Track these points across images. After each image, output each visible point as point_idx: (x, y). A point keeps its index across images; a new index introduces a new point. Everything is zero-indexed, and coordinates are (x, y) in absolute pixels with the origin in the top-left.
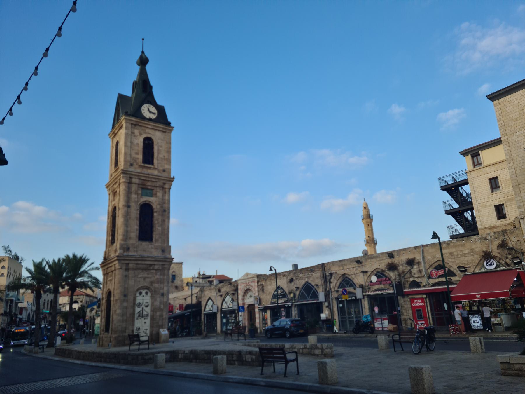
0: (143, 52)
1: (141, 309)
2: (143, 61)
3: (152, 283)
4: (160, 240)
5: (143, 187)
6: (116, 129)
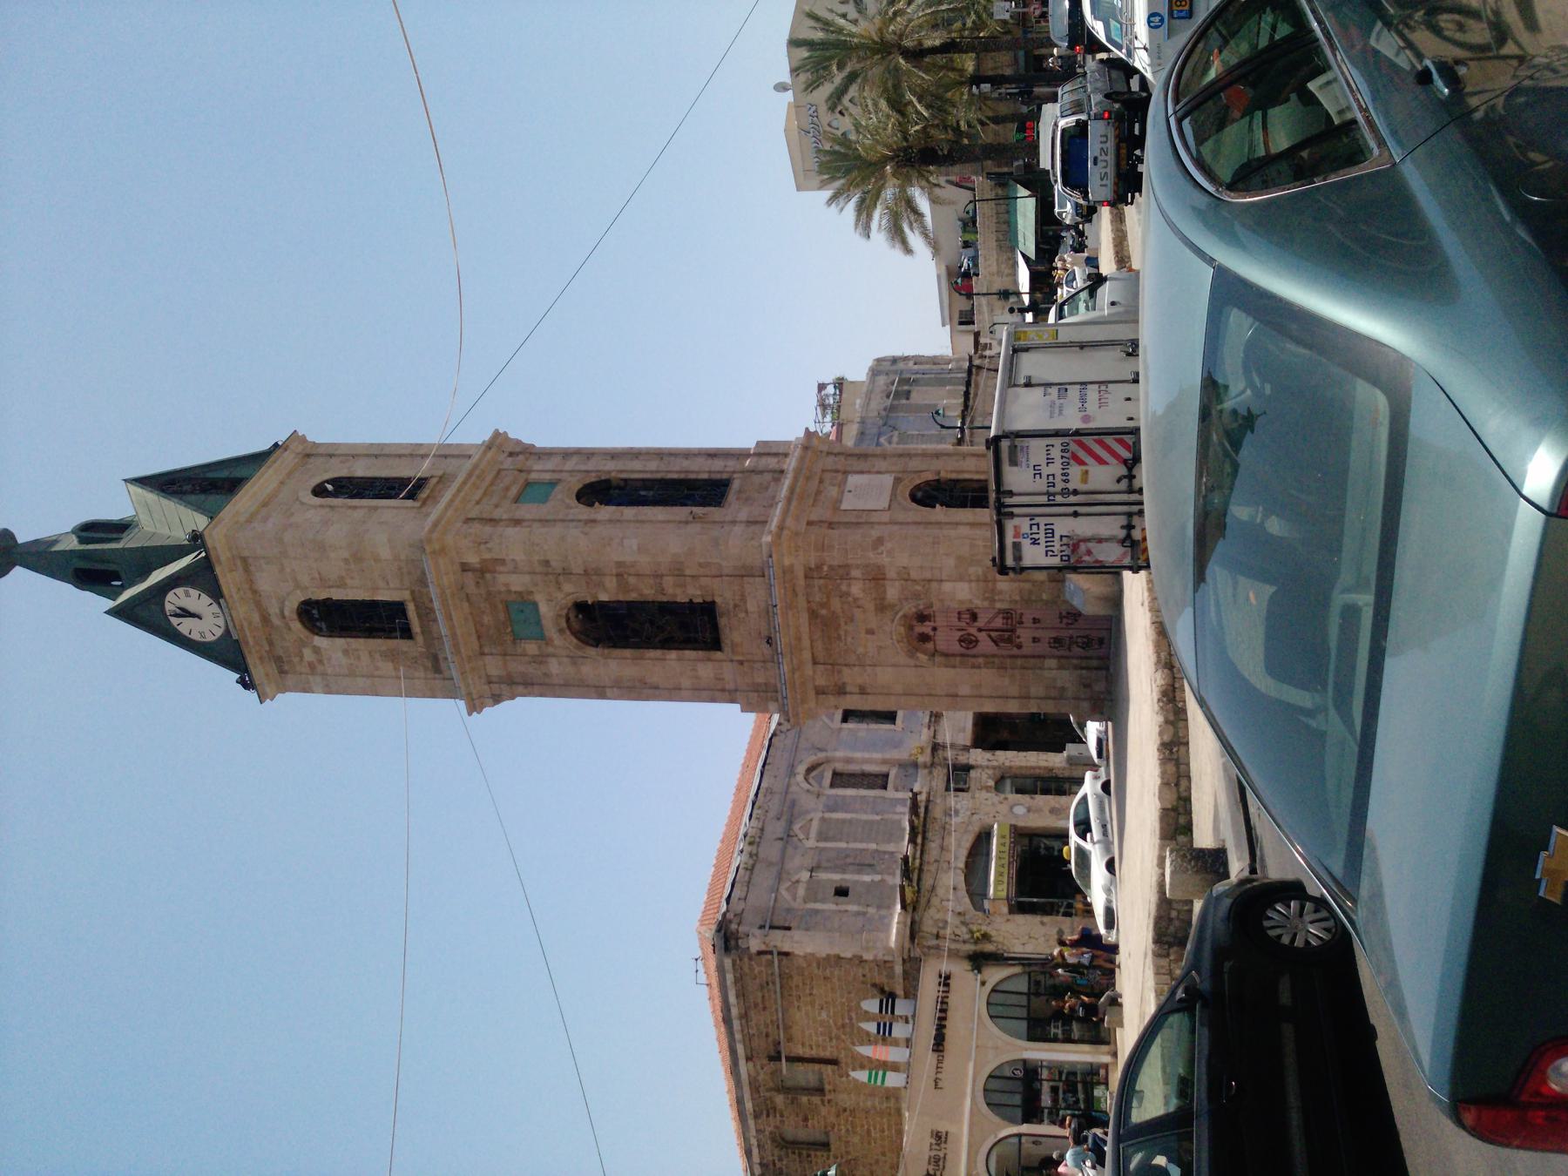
3: (882, 607)
5: (508, 638)
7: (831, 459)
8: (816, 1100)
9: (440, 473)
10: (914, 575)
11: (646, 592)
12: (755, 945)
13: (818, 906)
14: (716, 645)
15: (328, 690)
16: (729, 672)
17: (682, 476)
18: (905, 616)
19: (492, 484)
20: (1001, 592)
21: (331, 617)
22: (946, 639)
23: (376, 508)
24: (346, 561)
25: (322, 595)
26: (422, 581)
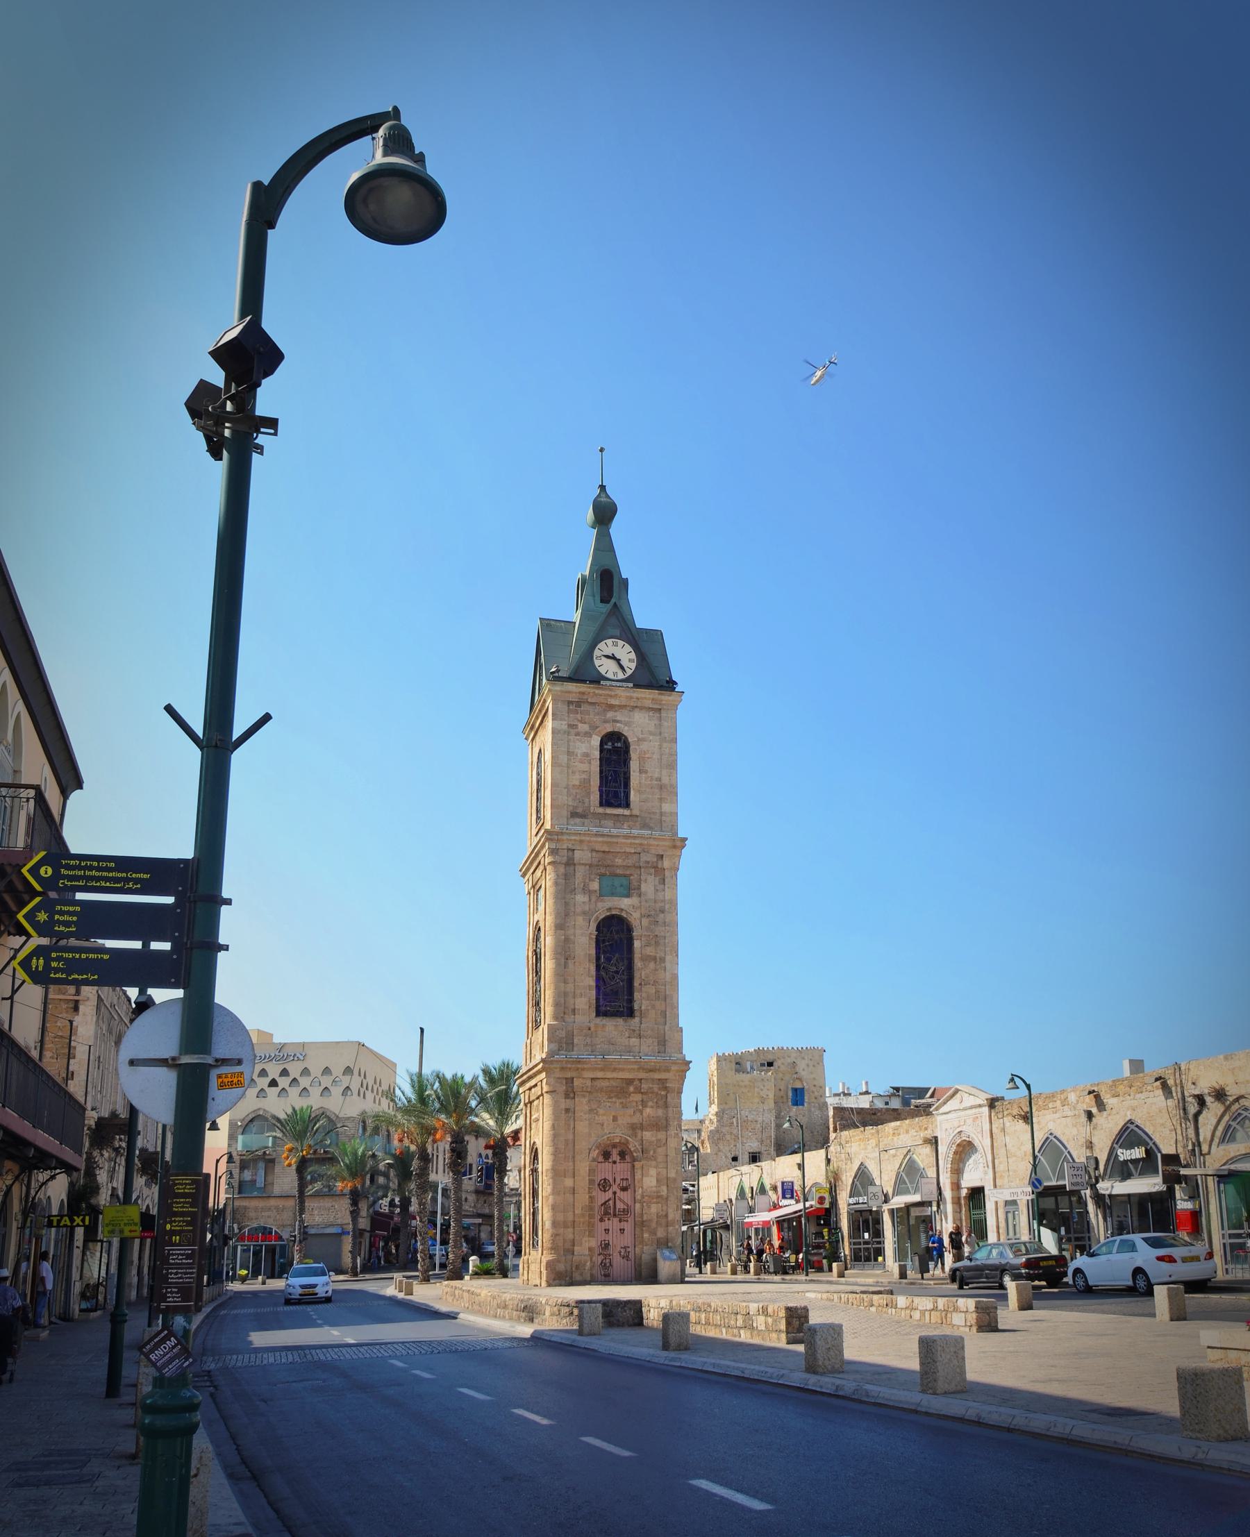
0: (602, 487)
1: (609, 1194)
2: (604, 513)
4: (652, 1014)
5: (603, 871)
6: (537, 718)
10: (659, 1150)
14: (598, 1014)
20: (649, 1207)
21: (615, 753)
25: (634, 755)
26: (645, 826)
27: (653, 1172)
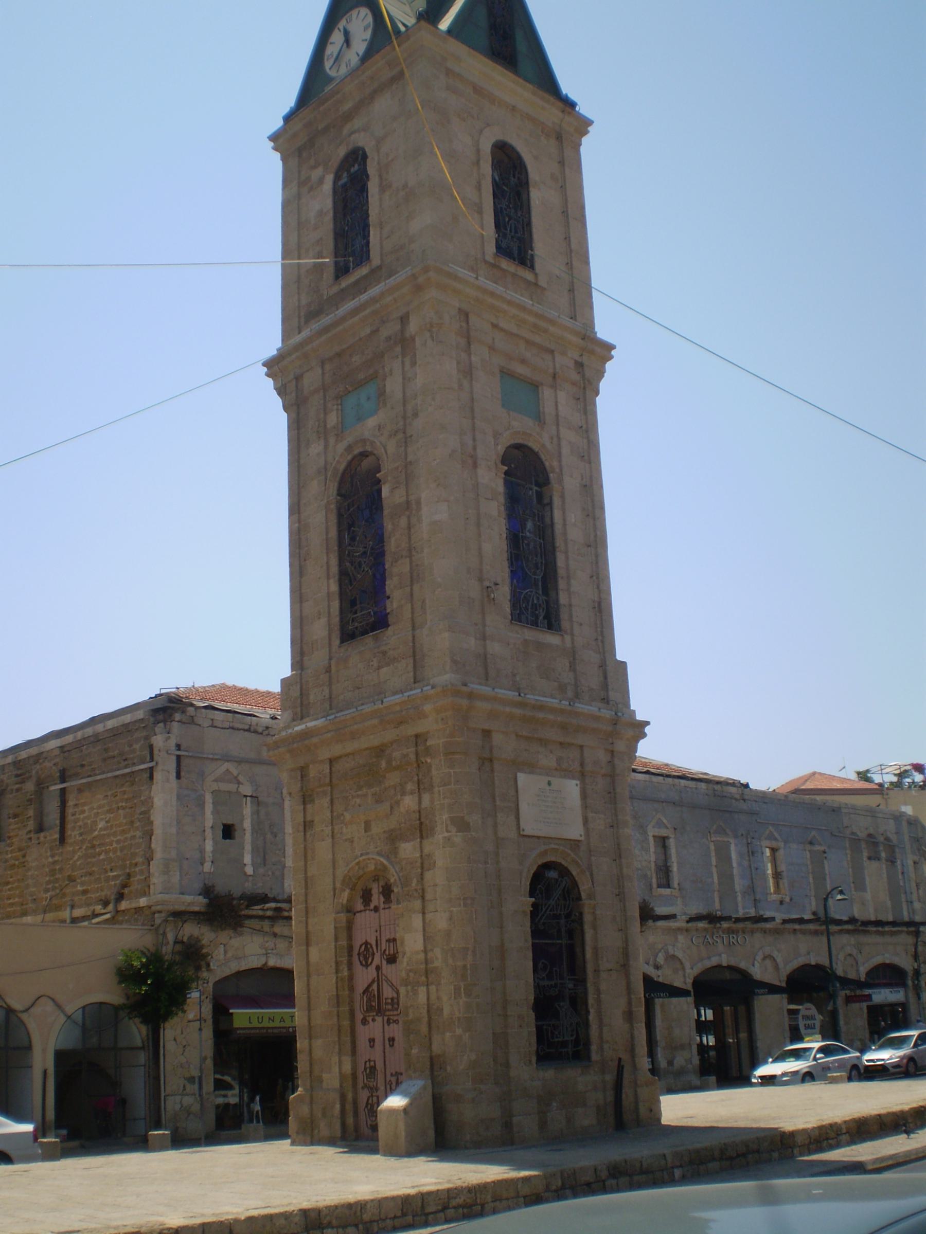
1: (372, 971)
3: (394, 838)
7: (603, 756)
8: (31, 825)
9: (542, 282)
10: (428, 875)
11: (393, 540)
12: (158, 741)
13: (209, 808)
15: (286, 205)
16: (318, 659)
17: (561, 572)
18: (385, 868)
19: (528, 342)
20: (415, 993)
22: (367, 927)
23: (480, 212)
24: (405, 186)
27: (417, 921)
